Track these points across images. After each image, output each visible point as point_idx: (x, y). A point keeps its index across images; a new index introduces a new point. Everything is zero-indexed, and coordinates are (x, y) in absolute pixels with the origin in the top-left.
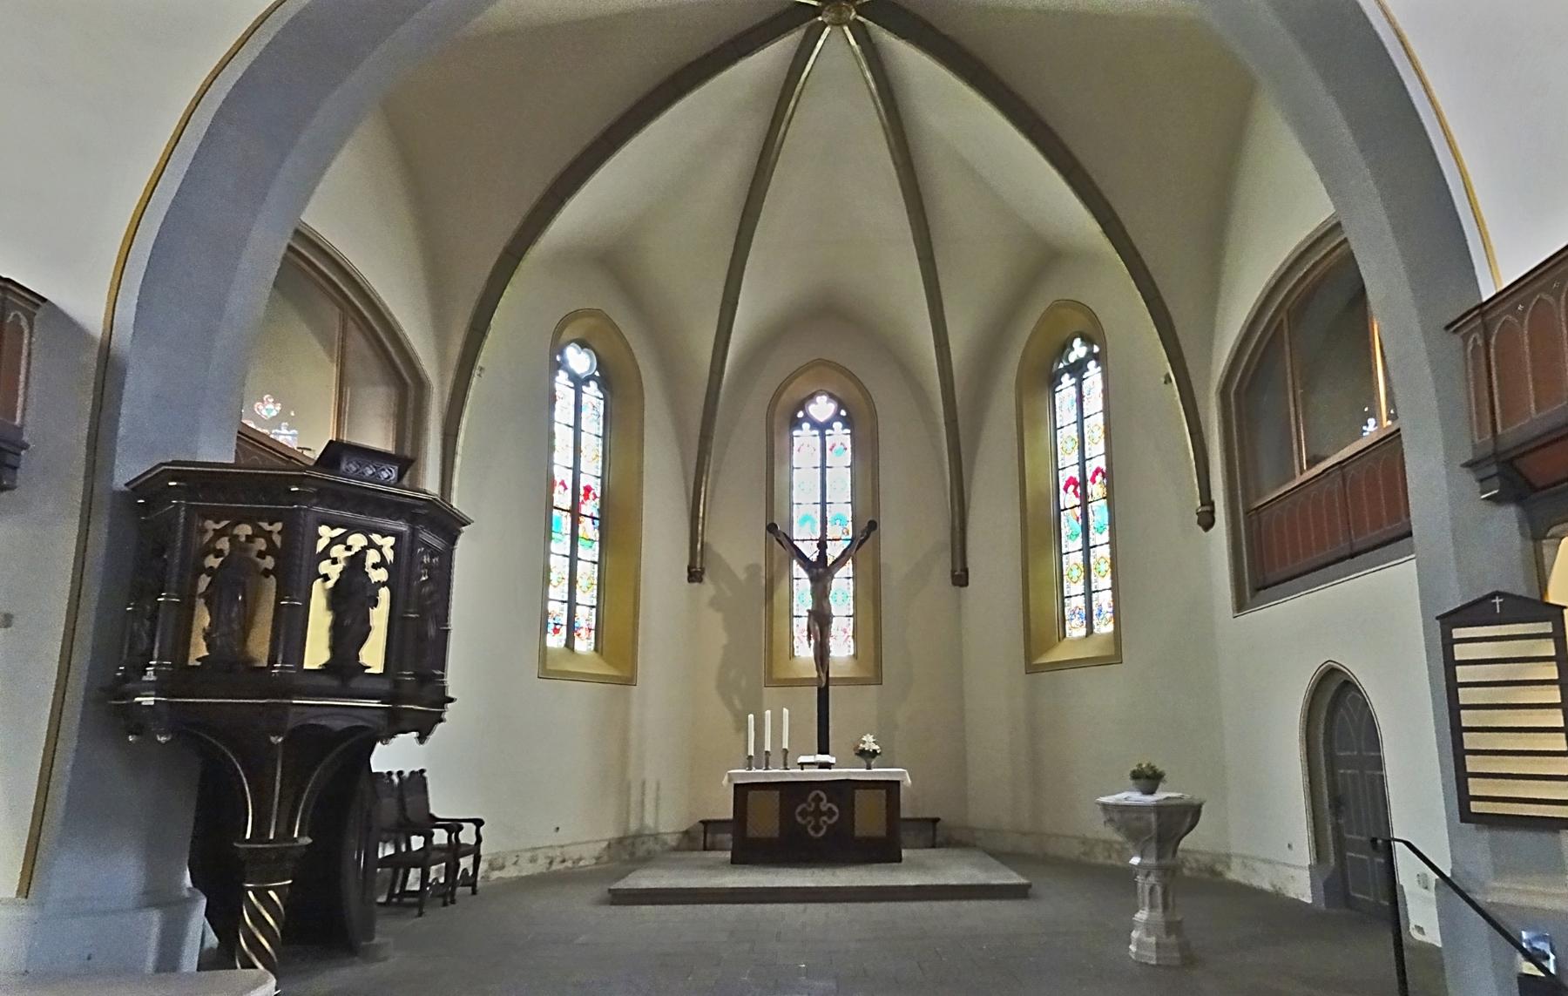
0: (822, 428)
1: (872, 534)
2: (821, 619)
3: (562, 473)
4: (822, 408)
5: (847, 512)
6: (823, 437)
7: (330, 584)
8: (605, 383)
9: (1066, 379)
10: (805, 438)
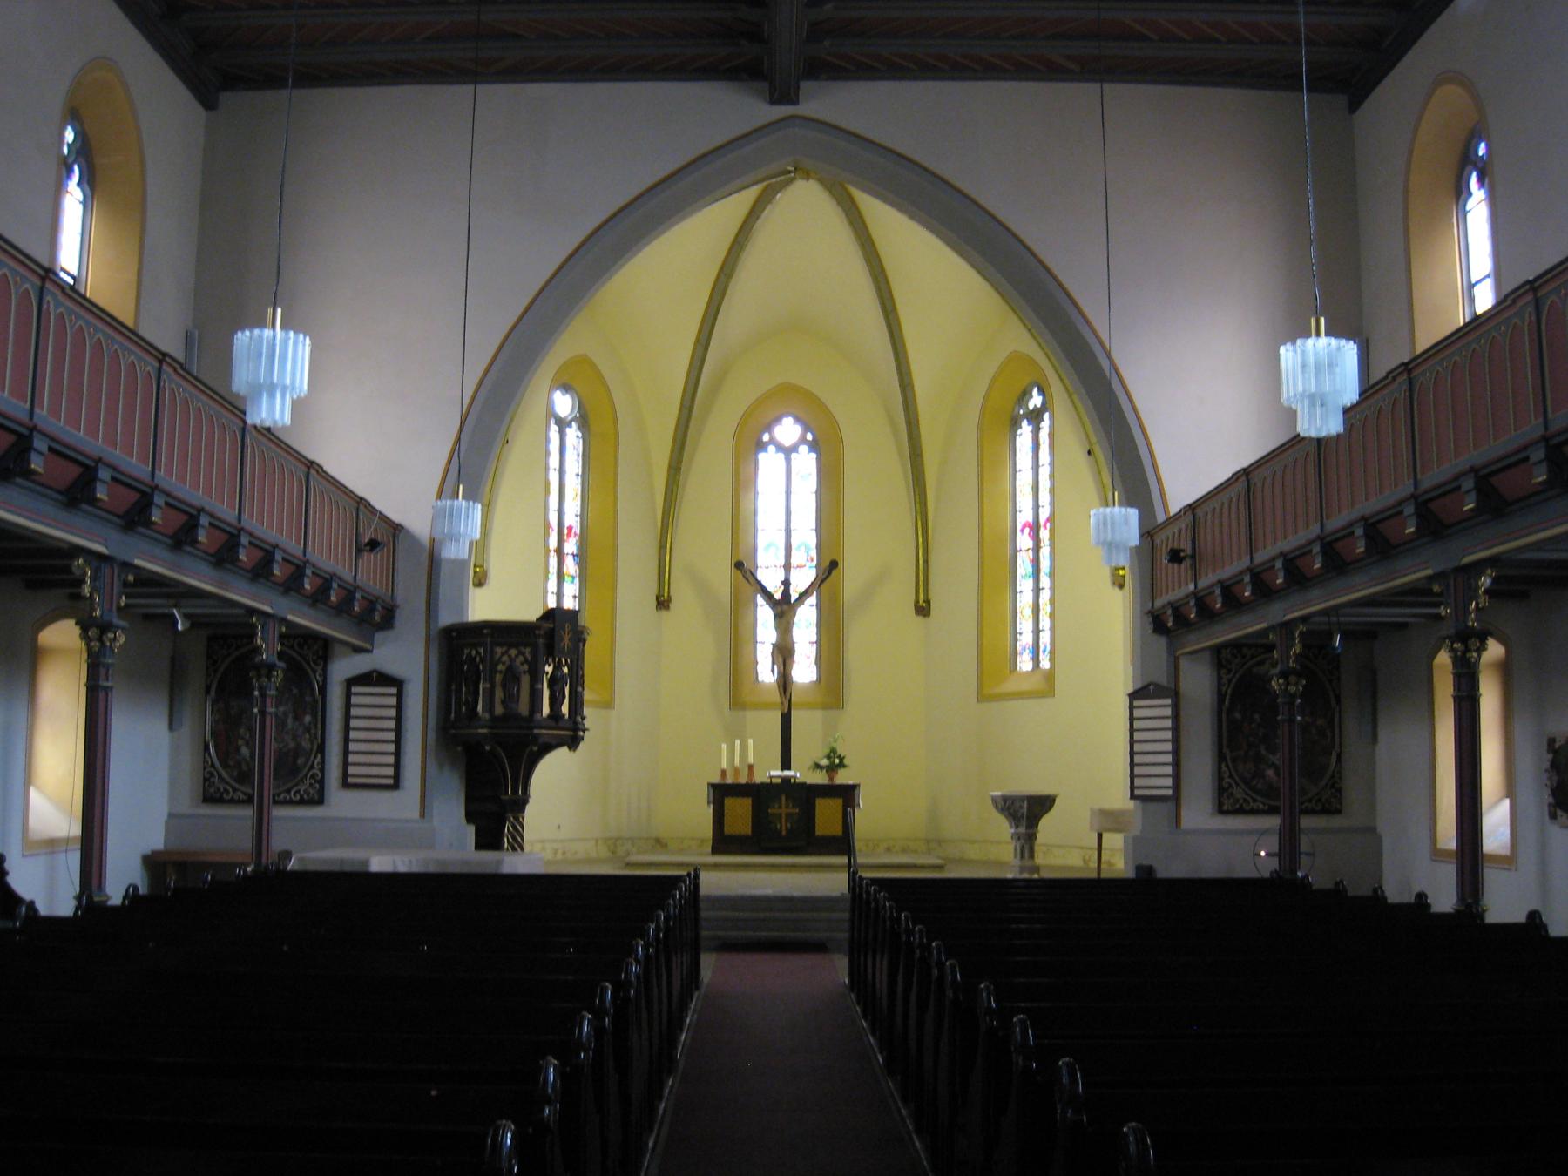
0: (788, 452)
1: (834, 573)
2: (784, 653)
3: (553, 519)
4: (788, 430)
5: (812, 540)
6: (788, 460)
7: (549, 676)
8: (584, 422)
9: (1025, 423)
10: (769, 464)
